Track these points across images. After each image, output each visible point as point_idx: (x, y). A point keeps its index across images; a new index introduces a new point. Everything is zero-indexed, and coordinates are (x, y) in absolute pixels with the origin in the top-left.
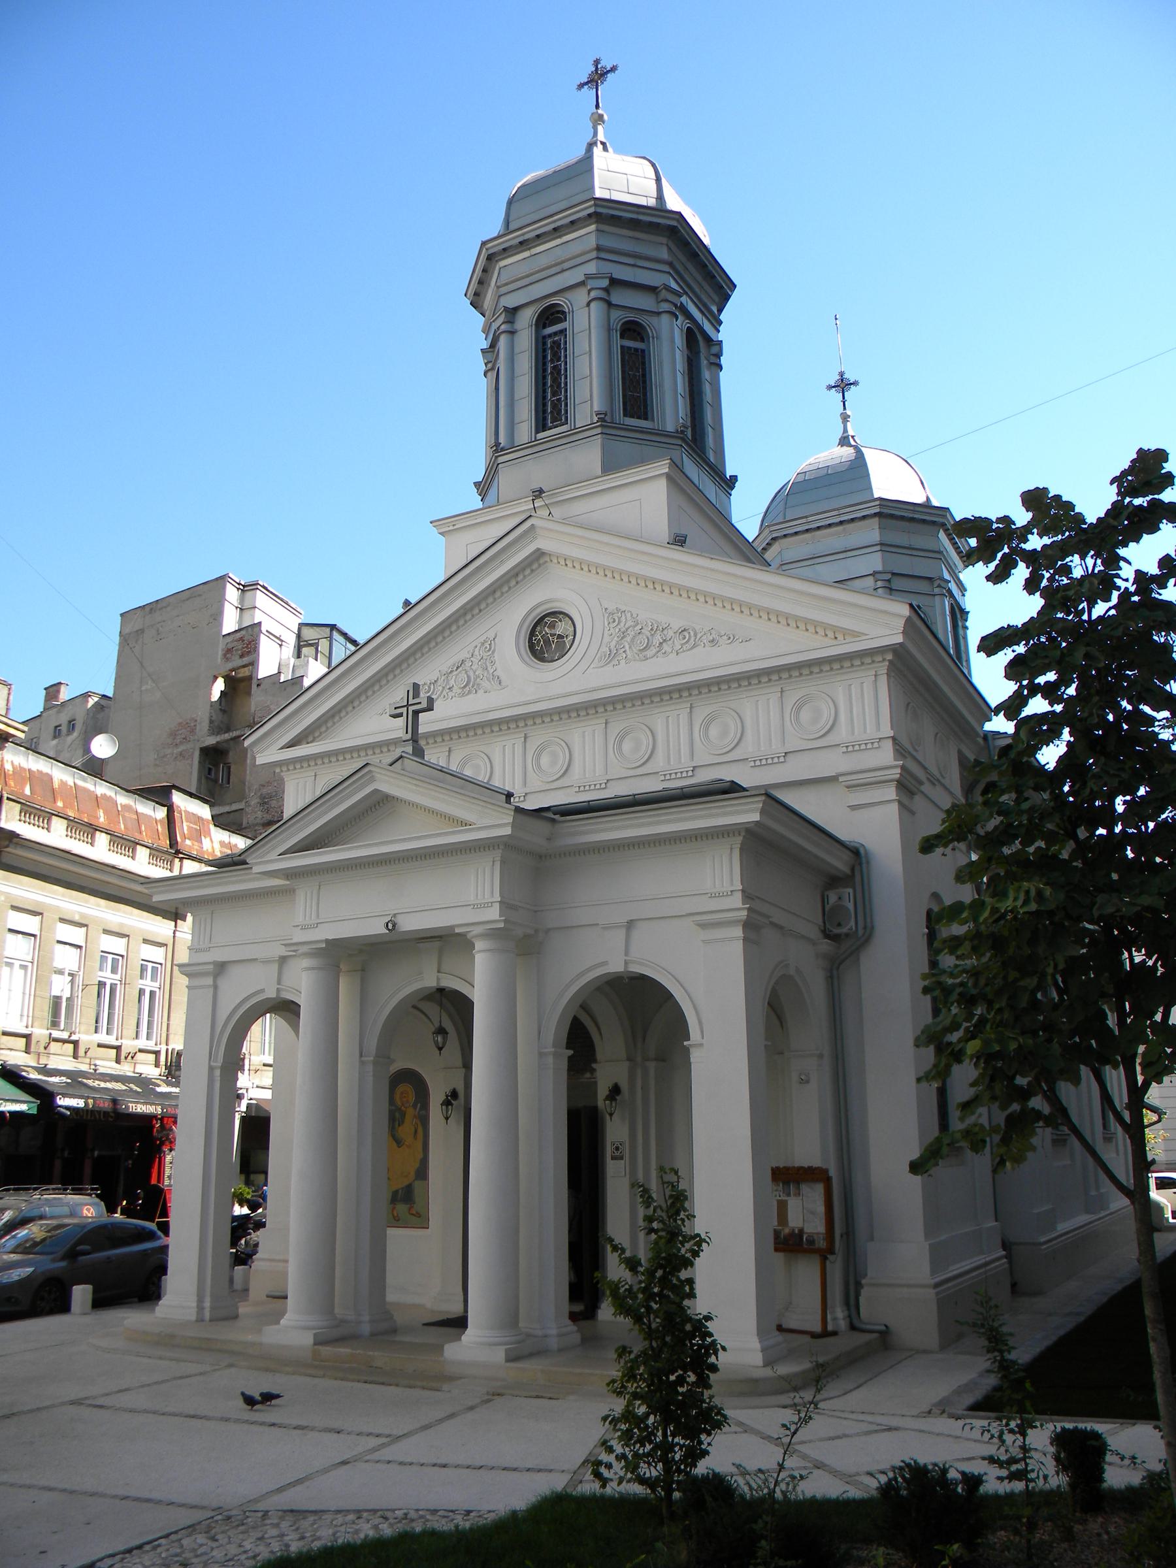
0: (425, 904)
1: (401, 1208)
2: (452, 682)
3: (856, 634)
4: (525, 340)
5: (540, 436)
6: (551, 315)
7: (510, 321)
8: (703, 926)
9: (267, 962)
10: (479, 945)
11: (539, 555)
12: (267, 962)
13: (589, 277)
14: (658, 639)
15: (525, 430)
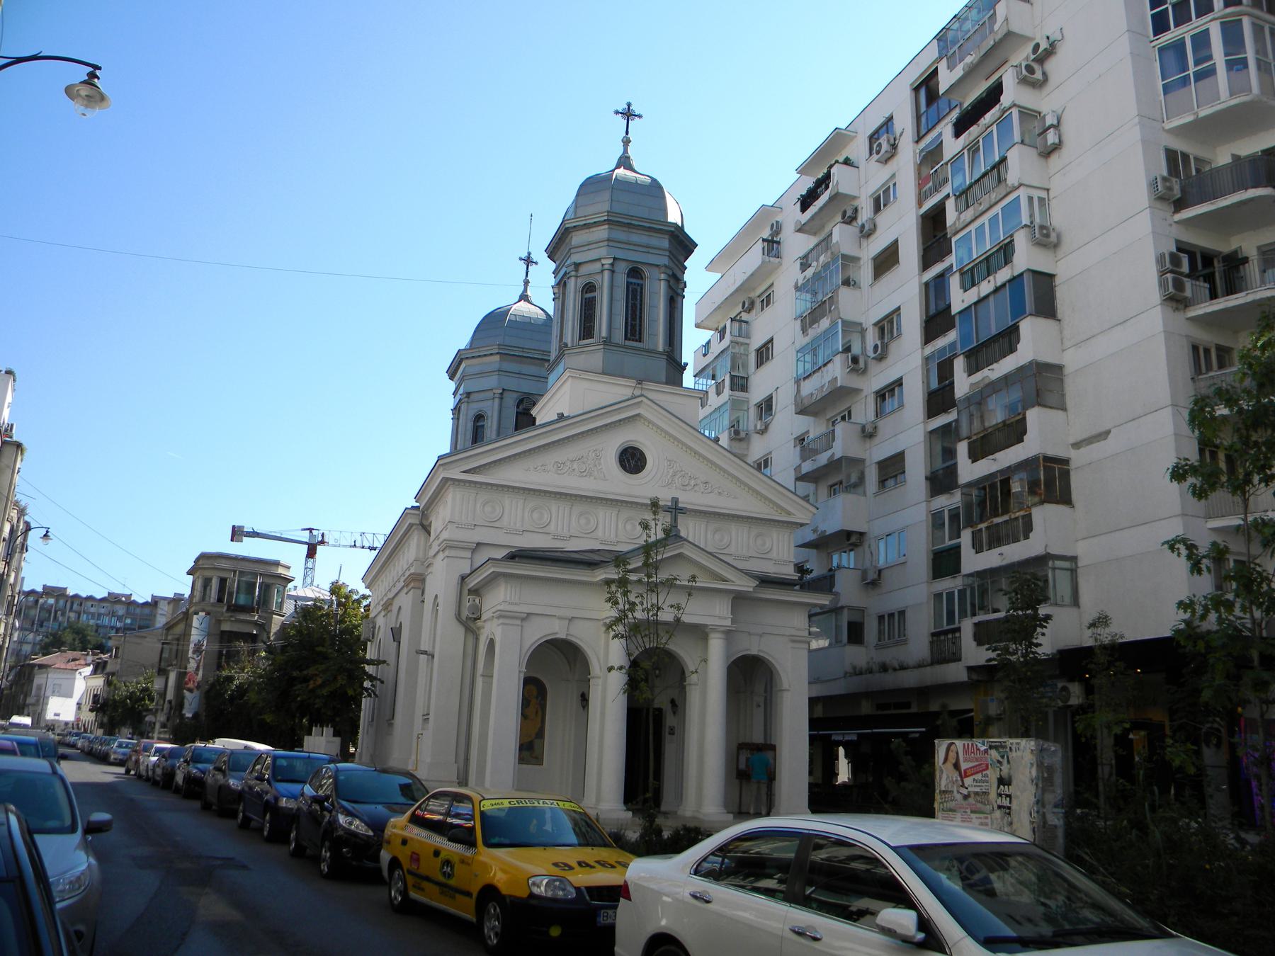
0: (695, 612)
1: (526, 754)
2: (575, 466)
3: (789, 513)
4: (622, 280)
5: (628, 343)
6: (635, 272)
7: (612, 265)
8: (794, 641)
9: (560, 618)
10: (712, 635)
11: (638, 415)
12: (560, 618)
13: (666, 266)
14: (693, 483)
15: (619, 336)
